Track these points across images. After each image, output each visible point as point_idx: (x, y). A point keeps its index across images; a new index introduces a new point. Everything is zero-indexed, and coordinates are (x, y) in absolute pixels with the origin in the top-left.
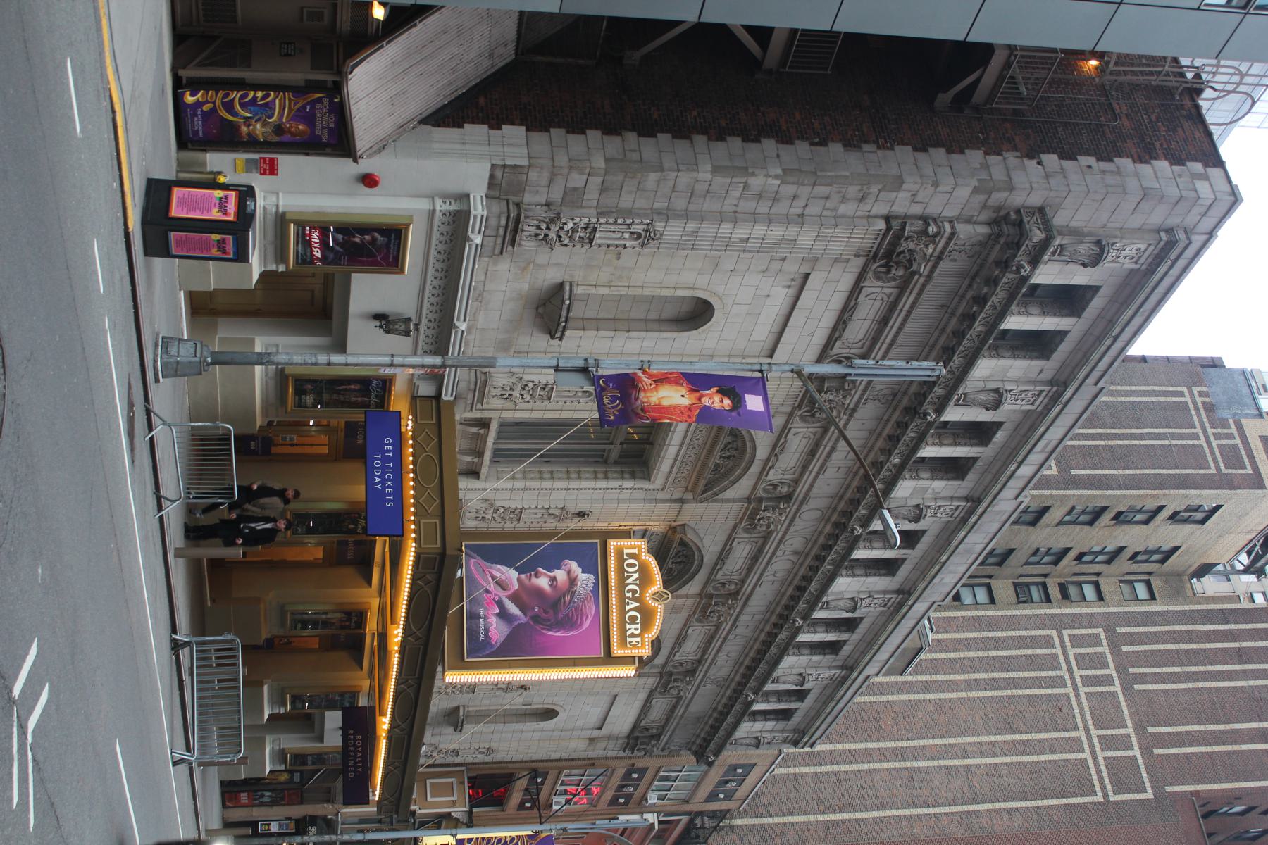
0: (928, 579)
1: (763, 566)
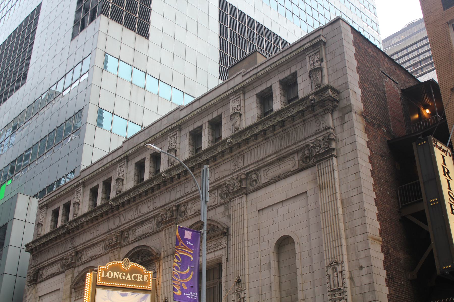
0: (154, 137)
1: (146, 216)
